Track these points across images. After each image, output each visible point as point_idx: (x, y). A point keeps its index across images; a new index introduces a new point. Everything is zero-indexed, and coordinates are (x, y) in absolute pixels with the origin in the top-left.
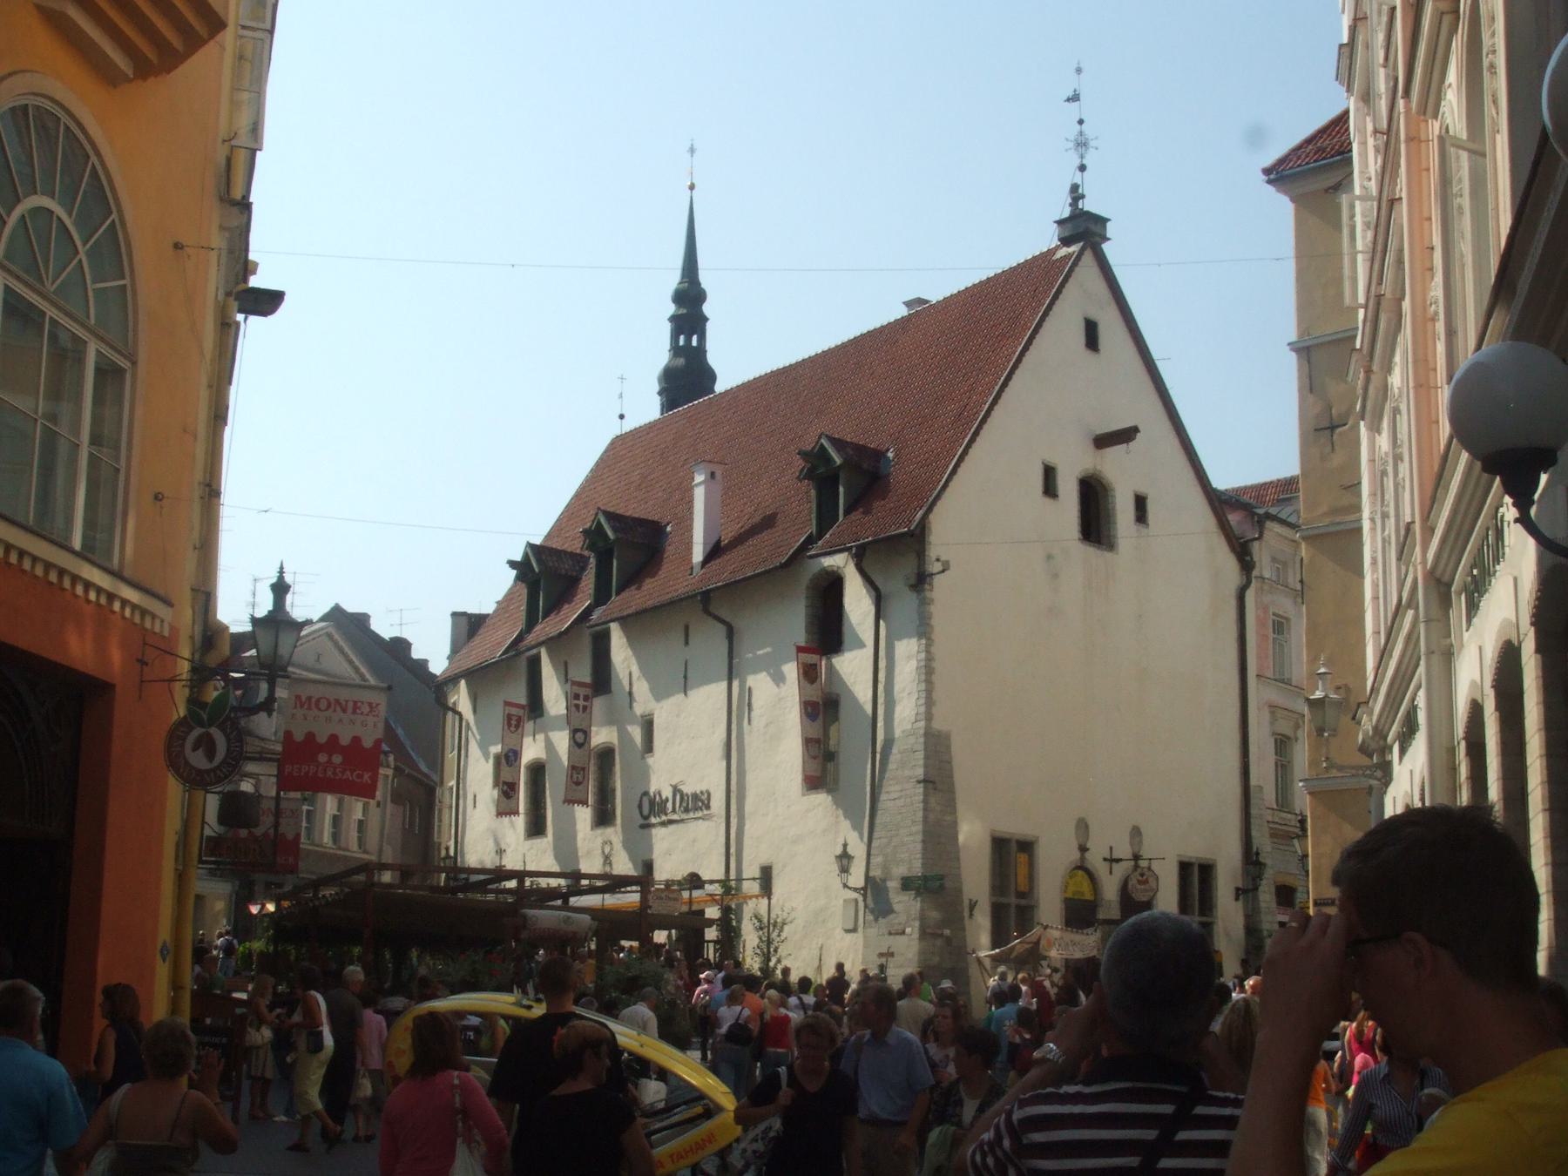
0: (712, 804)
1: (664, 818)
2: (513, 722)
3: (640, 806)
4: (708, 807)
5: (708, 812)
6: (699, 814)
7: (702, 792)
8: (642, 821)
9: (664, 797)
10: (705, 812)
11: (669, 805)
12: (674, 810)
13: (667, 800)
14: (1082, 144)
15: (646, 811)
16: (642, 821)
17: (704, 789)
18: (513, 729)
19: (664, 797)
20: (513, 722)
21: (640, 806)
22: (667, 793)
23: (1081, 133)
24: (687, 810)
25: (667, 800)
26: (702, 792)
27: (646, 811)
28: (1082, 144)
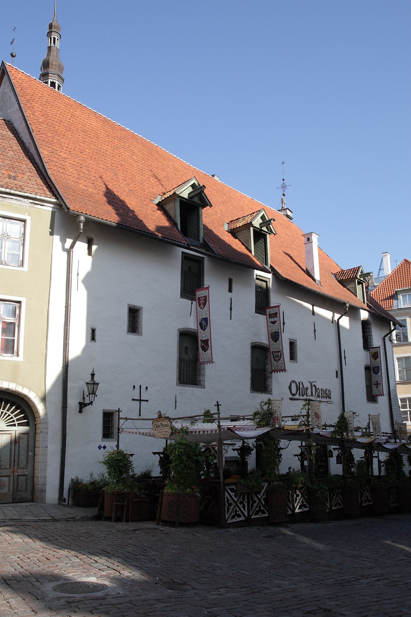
0: (332, 396)
1: (305, 397)
2: (202, 302)
3: (290, 388)
4: (330, 398)
5: (330, 400)
6: (325, 400)
7: (326, 390)
8: (291, 396)
9: (305, 387)
10: (328, 399)
11: (309, 391)
12: (312, 395)
13: (307, 389)
14: (284, 187)
15: (294, 391)
16: (291, 396)
17: (328, 389)
18: (202, 306)
19: (305, 387)
20: (202, 302)
21: (290, 388)
22: (307, 385)
23: (284, 183)
24: (318, 396)
25: (307, 389)
26: (326, 390)
27: (294, 390)
28: (284, 187)
